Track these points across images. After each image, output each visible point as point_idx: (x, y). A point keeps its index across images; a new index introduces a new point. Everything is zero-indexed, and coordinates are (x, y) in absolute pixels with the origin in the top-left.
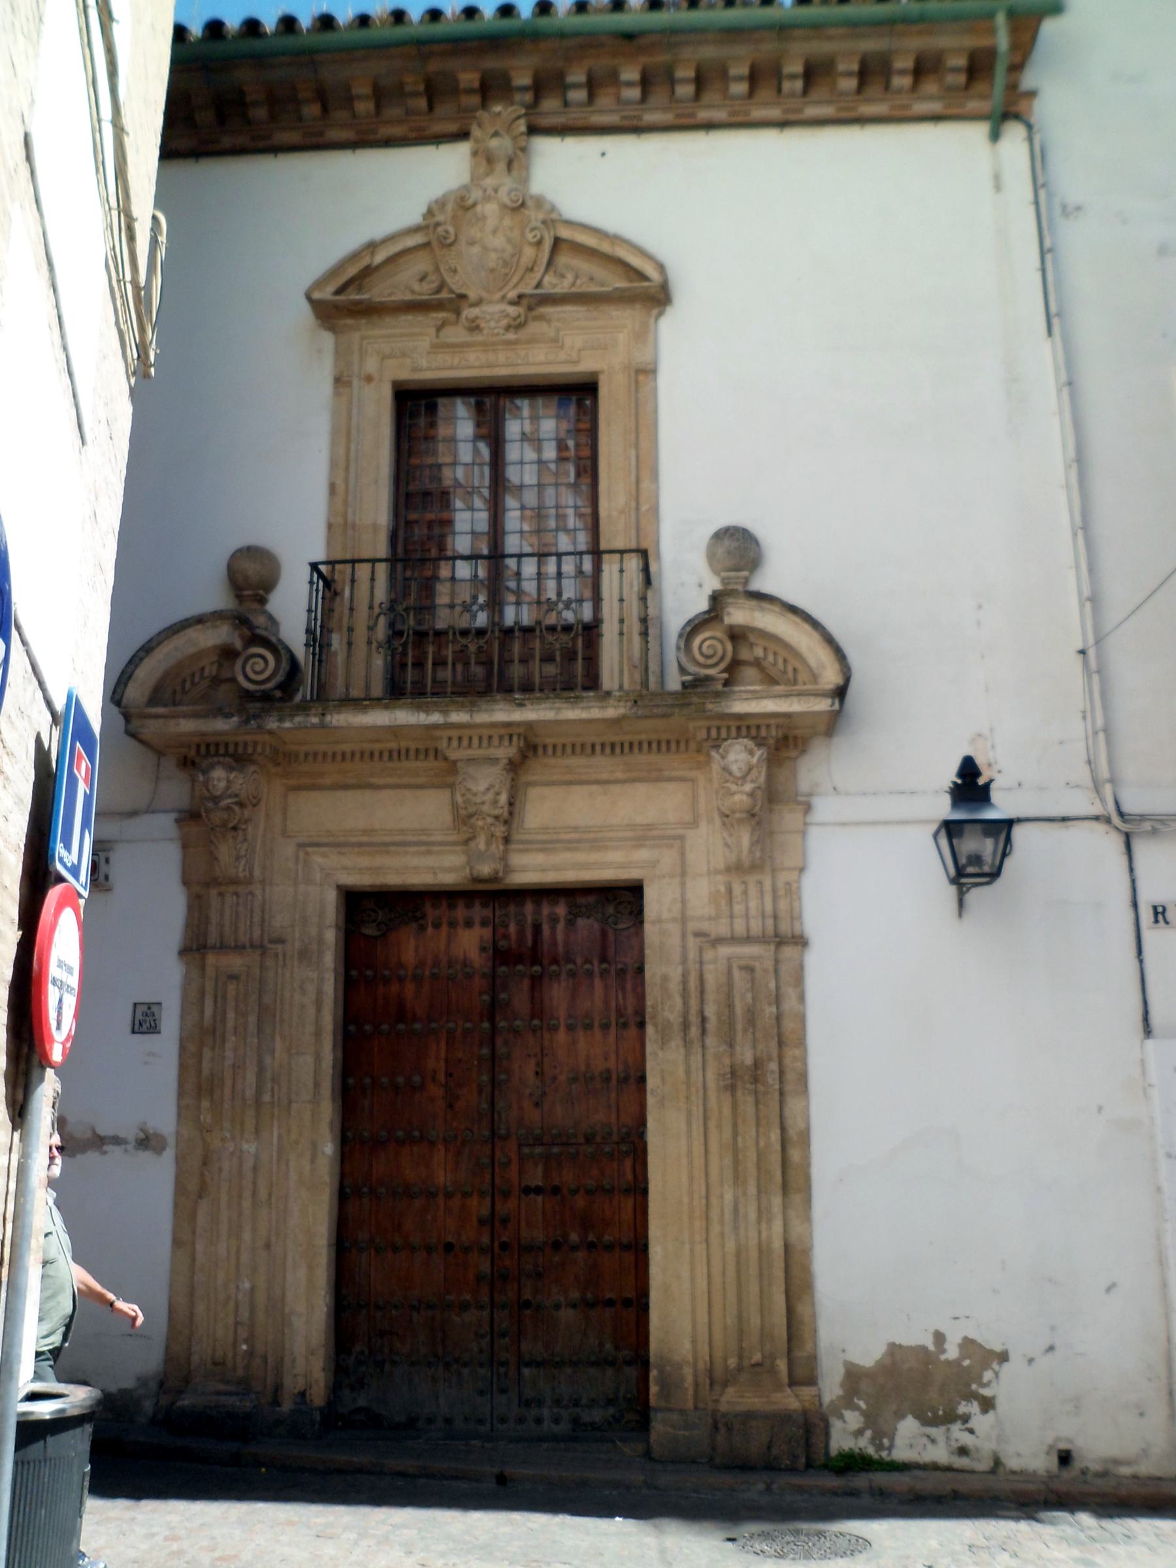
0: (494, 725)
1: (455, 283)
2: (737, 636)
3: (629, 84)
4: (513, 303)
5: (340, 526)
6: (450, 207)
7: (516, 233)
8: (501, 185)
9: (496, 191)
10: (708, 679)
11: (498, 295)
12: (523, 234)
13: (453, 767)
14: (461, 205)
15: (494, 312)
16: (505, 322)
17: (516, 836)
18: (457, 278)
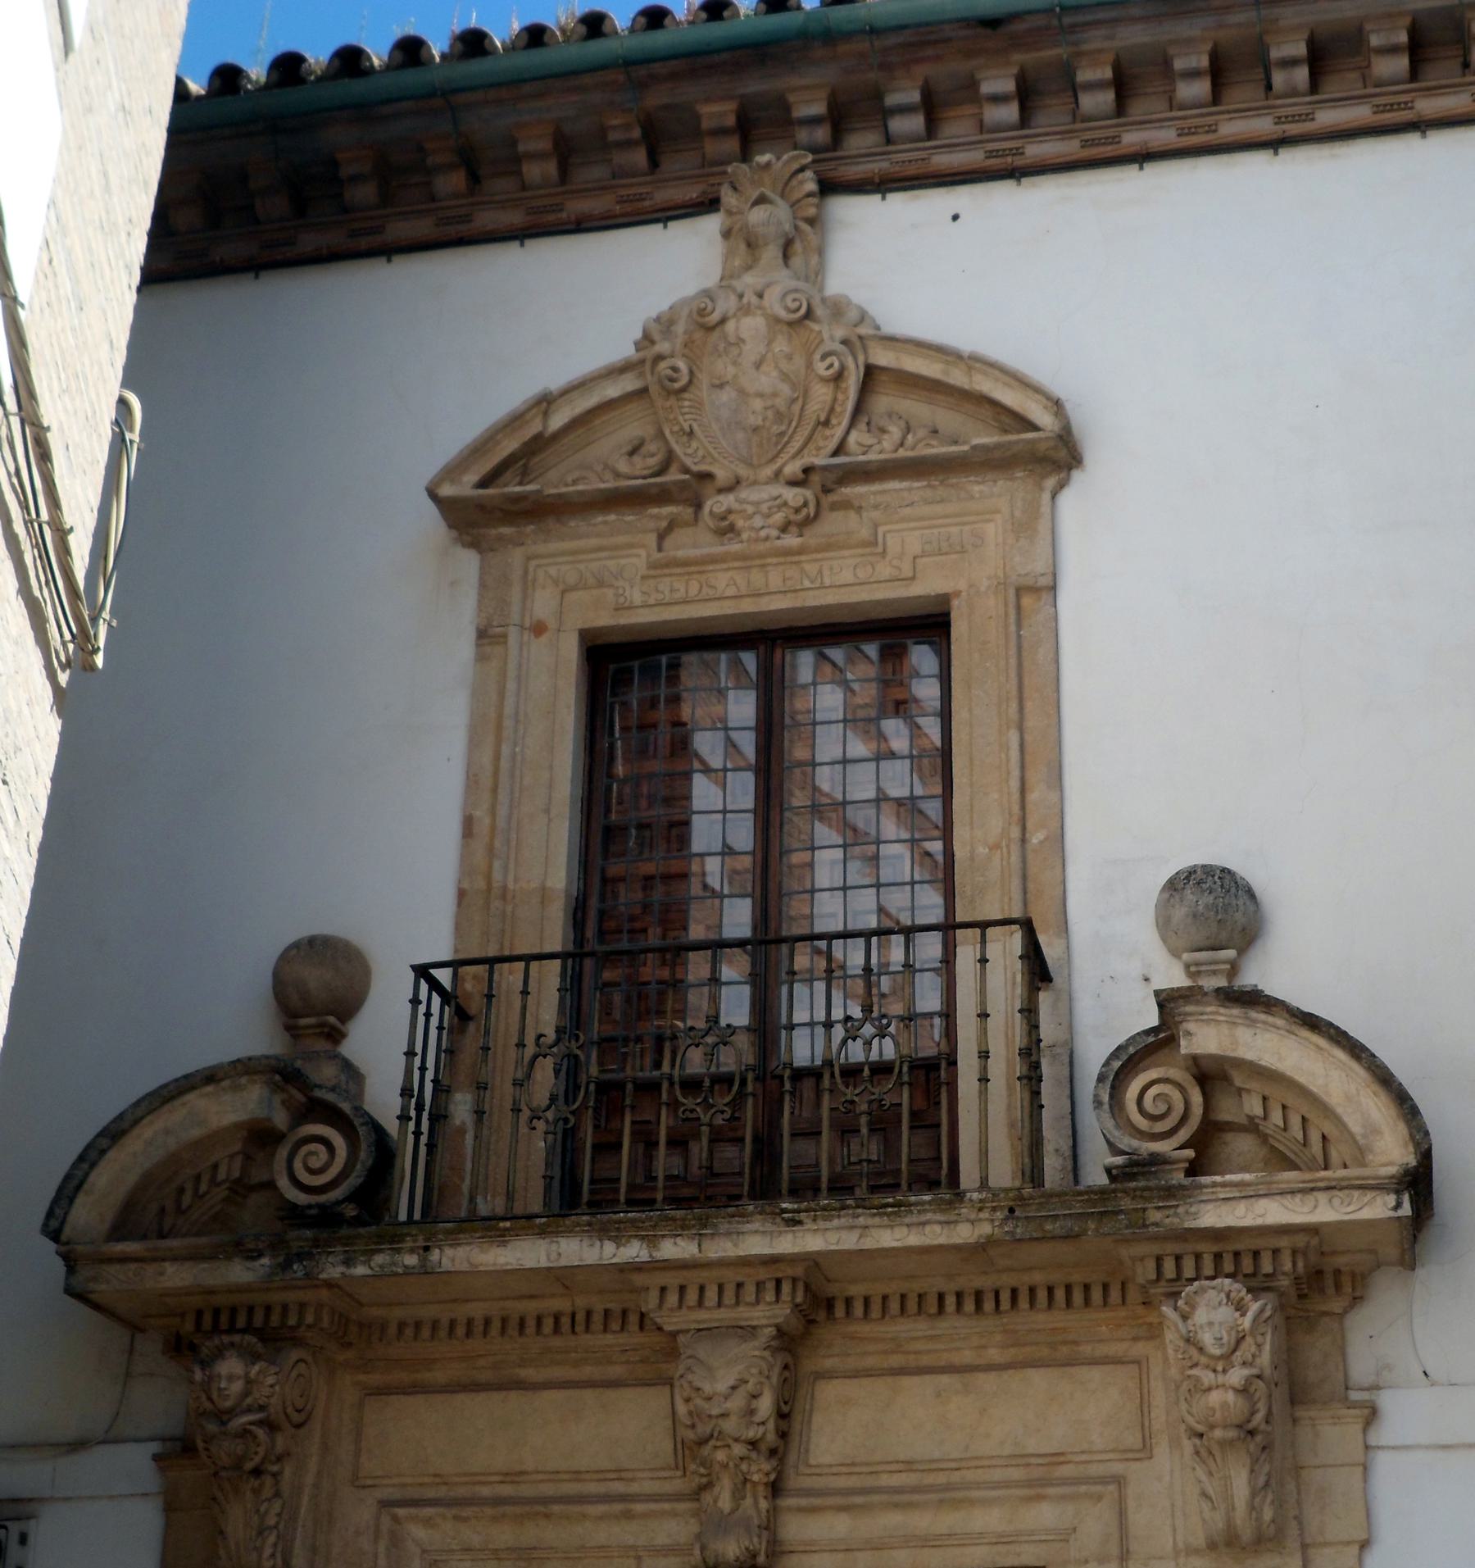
0: (746, 1262)
1: (691, 456)
2: (1210, 1076)
3: (997, 99)
4: (793, 483)
5: (476, 897)
6: (680, 328)
7: (799, 361)
8: (768, 285)
9: (760, 296)
10: (1156, 1160)
11: (768, 471)
12: (809, 365)
13: (671, 1347)
14: (702, 323)
15: (762, 500)
16: (779, 518)
17: (793, 1481)
18: (694, 444)
